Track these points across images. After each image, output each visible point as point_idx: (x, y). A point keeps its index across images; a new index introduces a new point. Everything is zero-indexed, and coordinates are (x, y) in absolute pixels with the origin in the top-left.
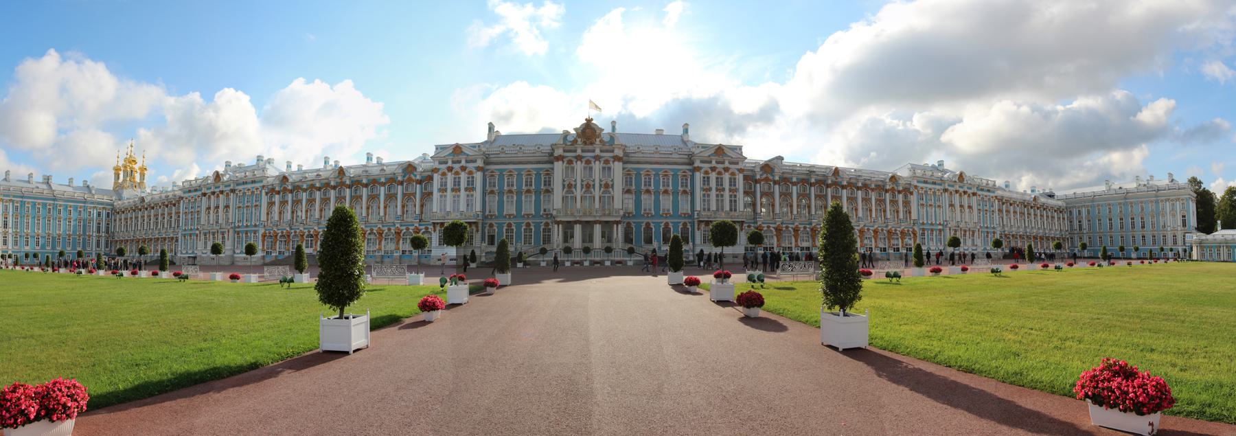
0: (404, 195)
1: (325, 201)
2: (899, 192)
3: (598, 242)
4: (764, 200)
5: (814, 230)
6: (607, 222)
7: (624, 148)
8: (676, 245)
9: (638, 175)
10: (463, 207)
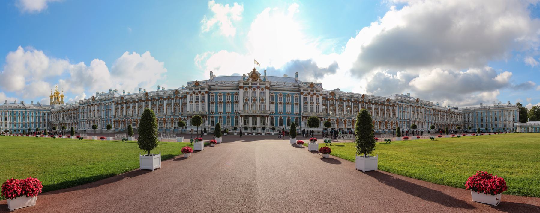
0: (174, 104)
1: (140, 107)
2: (391, 106)
3: (259, 125)
4: (331, 108)
5: (353, 121)
6: (263, 116)
7: (270, 83)
8: (293, 127)
9: (276, 96)
10: (200, 109)
